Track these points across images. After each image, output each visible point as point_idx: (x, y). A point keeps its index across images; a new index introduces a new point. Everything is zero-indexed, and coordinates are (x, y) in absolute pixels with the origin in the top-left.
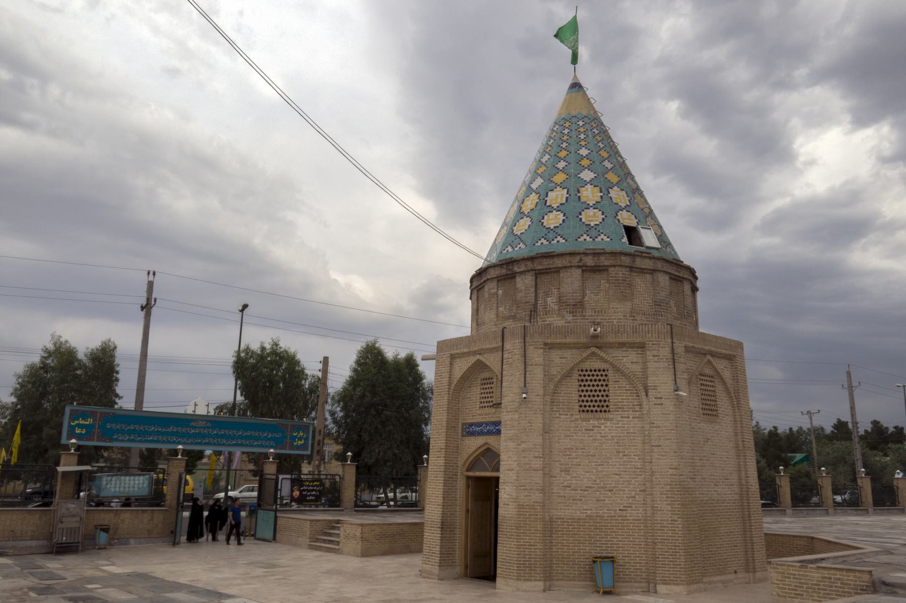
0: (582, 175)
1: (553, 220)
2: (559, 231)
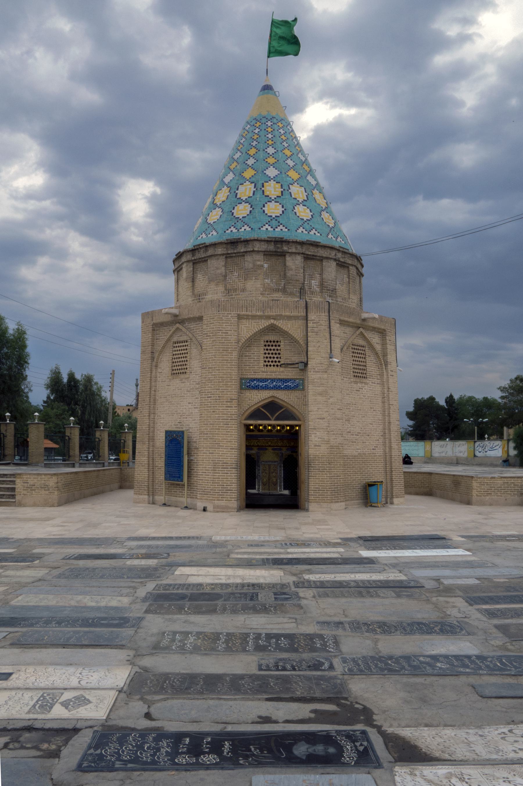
0: (268, 172)
1: (242, 210)
2: (245, 220)
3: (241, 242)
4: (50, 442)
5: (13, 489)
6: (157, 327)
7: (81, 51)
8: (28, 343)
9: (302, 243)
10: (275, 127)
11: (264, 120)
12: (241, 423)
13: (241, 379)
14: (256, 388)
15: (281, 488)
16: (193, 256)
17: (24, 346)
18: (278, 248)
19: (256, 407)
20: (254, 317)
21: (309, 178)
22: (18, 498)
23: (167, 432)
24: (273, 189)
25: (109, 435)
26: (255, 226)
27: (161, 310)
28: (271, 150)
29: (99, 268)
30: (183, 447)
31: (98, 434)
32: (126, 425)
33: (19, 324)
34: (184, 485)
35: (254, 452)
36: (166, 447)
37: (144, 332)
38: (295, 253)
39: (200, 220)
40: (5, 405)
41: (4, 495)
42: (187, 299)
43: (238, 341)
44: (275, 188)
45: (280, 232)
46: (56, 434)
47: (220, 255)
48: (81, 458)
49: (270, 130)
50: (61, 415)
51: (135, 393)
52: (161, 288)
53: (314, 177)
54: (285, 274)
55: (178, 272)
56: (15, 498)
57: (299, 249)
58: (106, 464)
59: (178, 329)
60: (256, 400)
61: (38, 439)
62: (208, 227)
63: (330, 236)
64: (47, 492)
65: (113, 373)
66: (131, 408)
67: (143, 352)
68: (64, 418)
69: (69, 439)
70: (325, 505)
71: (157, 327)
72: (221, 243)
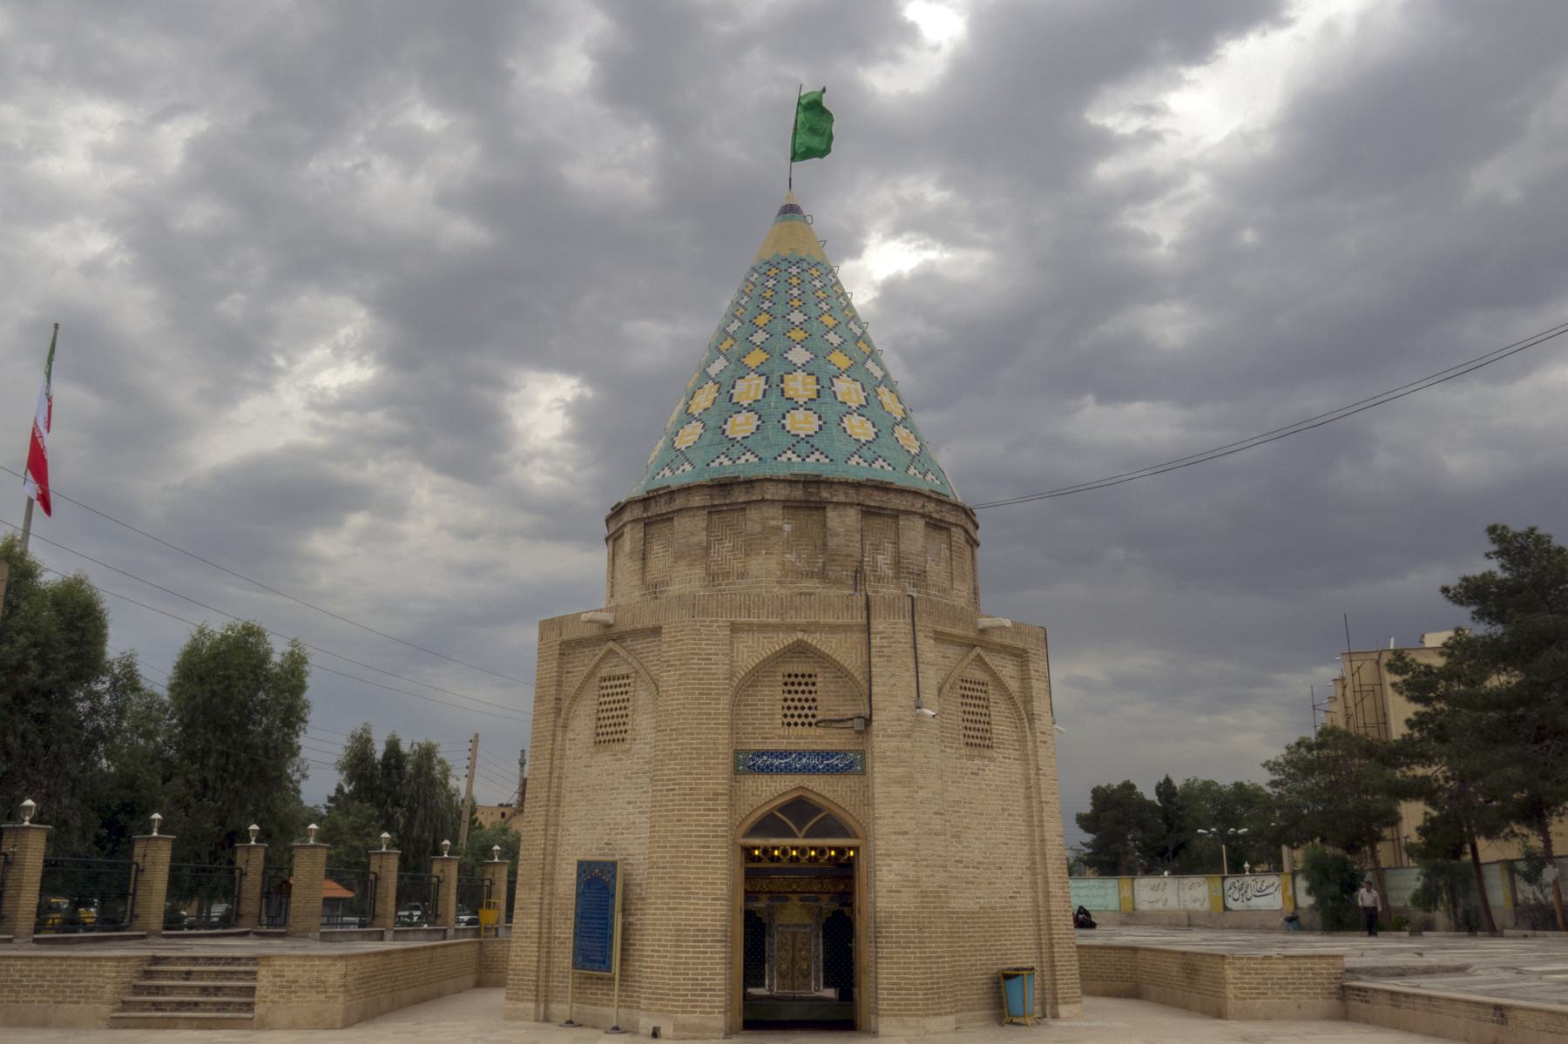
0: (791, 356)
1: (741, 425)
2: (748, 443)
3: (739, 483)
4: (335, 885)
5: (251, 991)
6: (569, 648)
7: (462, 159)
8: (309, 680)
9: (857, 486)
10: (806, 276)
11: (784, 265)
12: (734, 842)
13: (737, 752)
14: (768, 770)
15: (817, 985)
16: (646, 510)
17: (302, 687)
18: (811, 494)
19: (766, 809)
20: (763, 628)
21: (870, 365)
22: (259, 1009)
23: (581, 864)
24: (801, 387)
25: (461, 869)
26: (766, 454)
27: (579, 615)
28: (797, 317)
29: (467, 534)
30: (613, 896)
31: (436, 868)
32: (497, 847)
33: (294, 643)
34: (613, 979)
35: (761, 904)
36: (578, 895)
37: (542, 658)
38: (845, 504)
39: (661, 444)
40: (250, 808)
41: (229, 1004)
42: (631, 592)
43: (732, 675)
44: (805, 384)
45: (815, 464)
46: (350, 868)
47: (698, 508)
48: (399, 921)
49: (795, 281)
50: (364, 826)
51: (517, 781)
52: (580, 571)
53: (879, 364)
54: (825, 544)
55: (615, 540)
56: (252, 1010)
57: (853, 496)
58: (450, 932)
59: (611, 651)
60: (766, 796)
61: (311, 878)
62: (675, 456)
63: (912, 471)
64: (322, 997)
65: (475, 740)
66: (508, 811)
67: (539, 699)
68: (368, 835)
69: (377, 879)
70: (912, 1021)
71: (569, 648)
72: (700, 486)
